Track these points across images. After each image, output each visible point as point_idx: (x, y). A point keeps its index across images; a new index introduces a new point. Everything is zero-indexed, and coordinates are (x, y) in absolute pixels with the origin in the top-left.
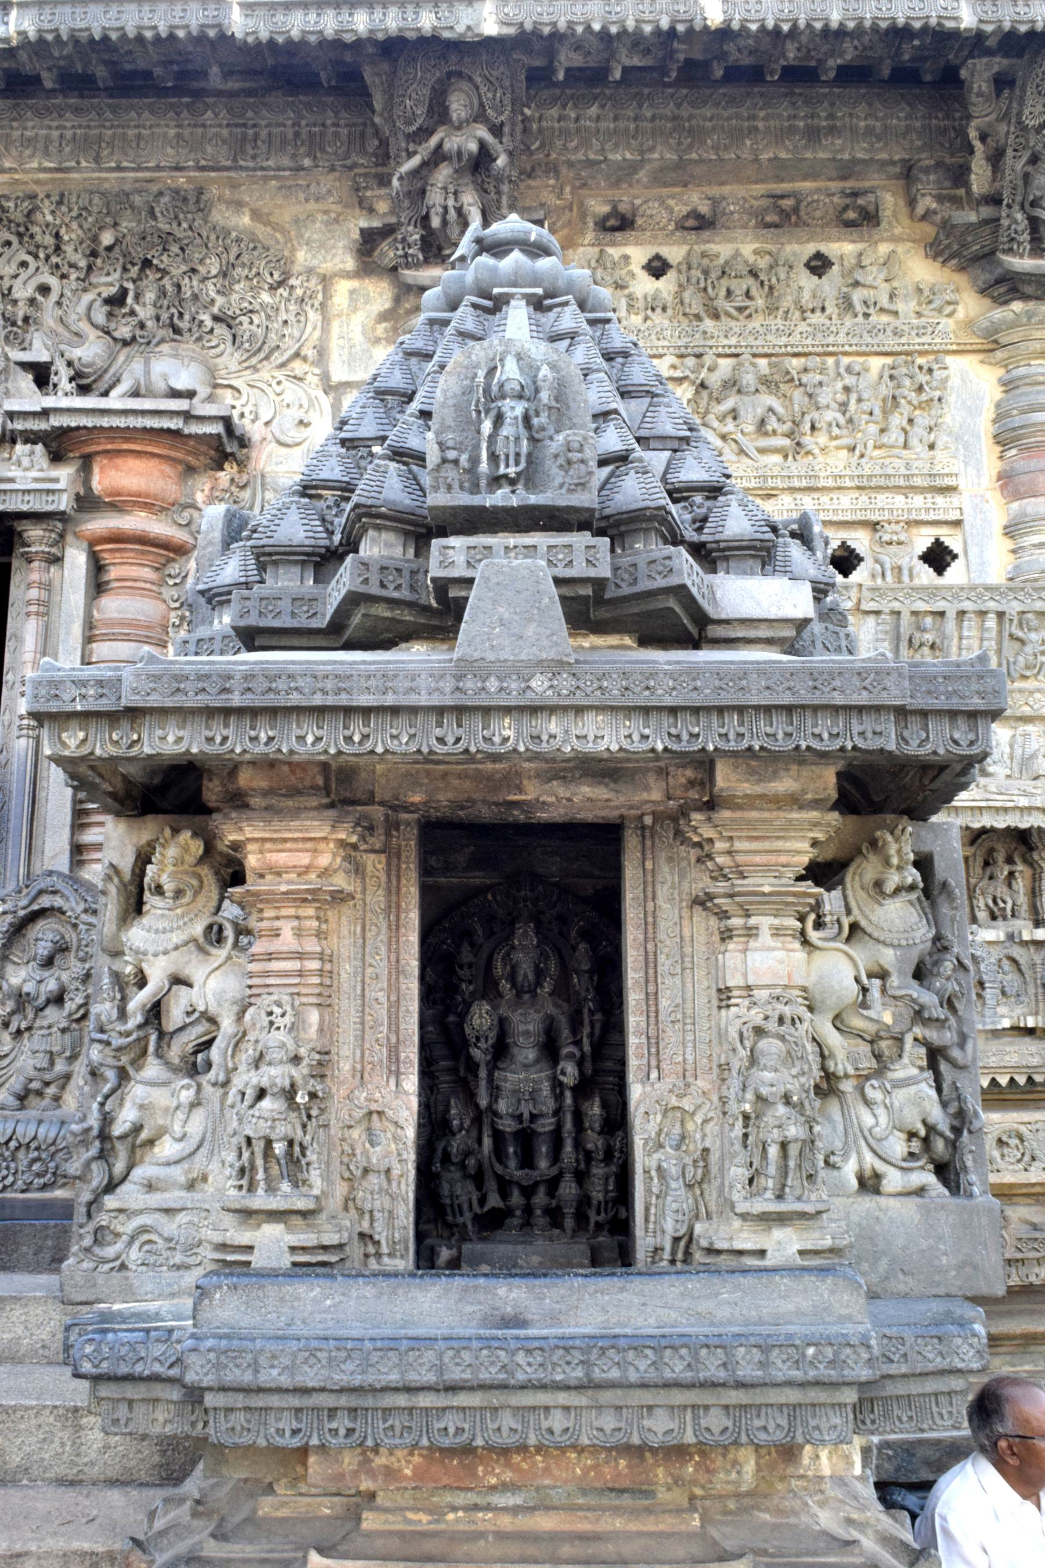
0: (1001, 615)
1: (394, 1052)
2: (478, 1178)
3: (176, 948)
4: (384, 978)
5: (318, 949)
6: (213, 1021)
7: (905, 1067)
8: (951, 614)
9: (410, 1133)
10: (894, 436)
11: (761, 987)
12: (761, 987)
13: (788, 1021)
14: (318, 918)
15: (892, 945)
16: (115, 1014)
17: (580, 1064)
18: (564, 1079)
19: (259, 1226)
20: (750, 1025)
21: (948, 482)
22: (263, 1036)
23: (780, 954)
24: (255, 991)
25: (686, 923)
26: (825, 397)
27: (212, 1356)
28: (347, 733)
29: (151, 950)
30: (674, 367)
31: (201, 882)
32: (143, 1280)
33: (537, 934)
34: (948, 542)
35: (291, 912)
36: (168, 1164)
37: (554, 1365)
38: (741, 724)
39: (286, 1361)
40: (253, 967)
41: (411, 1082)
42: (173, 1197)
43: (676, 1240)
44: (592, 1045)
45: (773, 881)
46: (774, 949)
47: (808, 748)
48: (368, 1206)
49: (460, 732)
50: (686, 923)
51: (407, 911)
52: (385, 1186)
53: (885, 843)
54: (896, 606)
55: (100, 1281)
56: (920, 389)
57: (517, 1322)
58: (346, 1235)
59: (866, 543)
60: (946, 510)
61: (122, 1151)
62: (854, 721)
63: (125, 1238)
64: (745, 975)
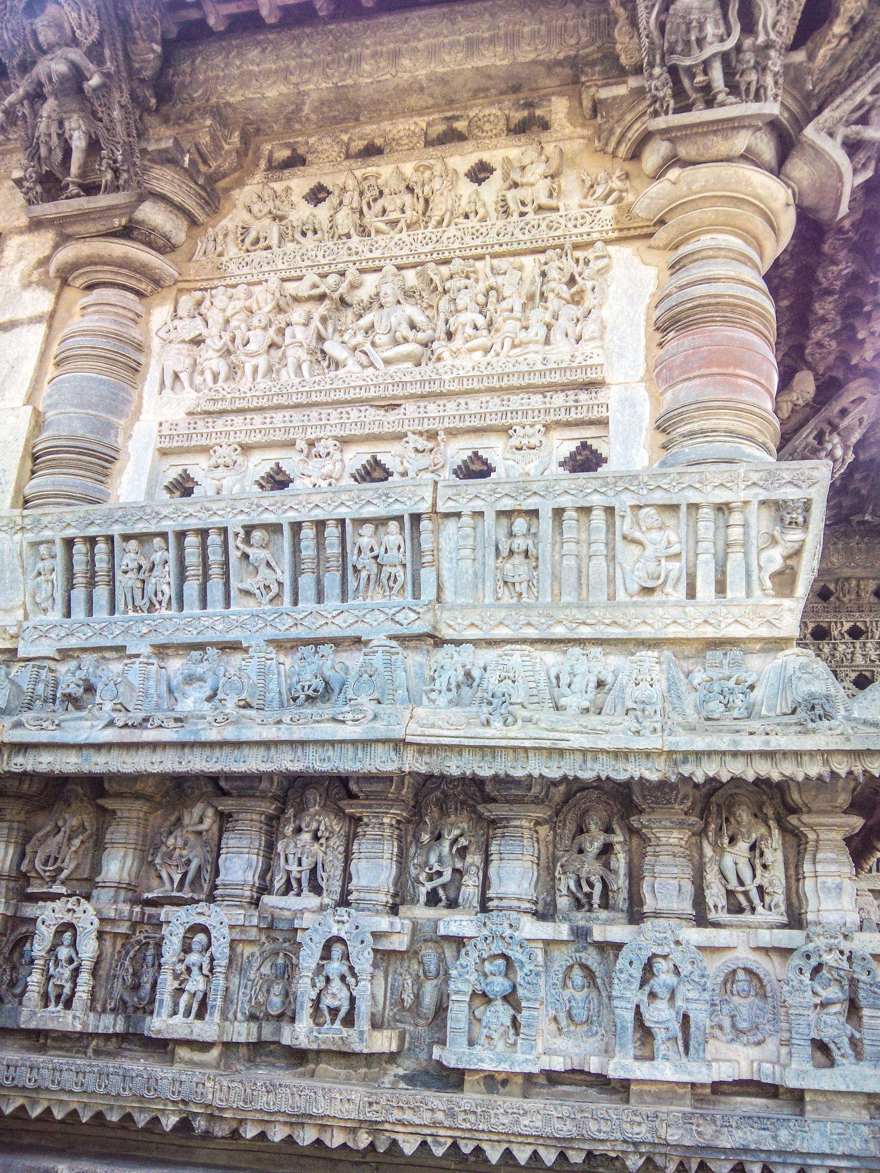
0: (610, 511)
8: (546, 514)
10: (537, 331)
21: (592, 376)
26: (463, 299)
30: (315, 286)
34: (595, 444)
54: (478, 505)
56: (572, 281)
59: (499, 451)
60: (590, 408)
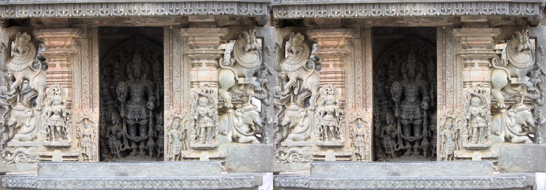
1: (91, 101)
2: (122, 139)
3: (24, 69)
4: (88, 78)
5: (67, 70)
6: (36, 91)
7: (248, 105)
9: (97, 125)
11: (202, 82)
12: (202, 82)
13: (209, 92)
14: (67, 61)
15: (246, 68)
16: (6, 90)
17: (155, 103)
18: (150, 108)
19: (53, 150)
20: (197, 93)
22: (52, 97)
23: (209, 72)
24: (49, 83)
25: (182, 61)
27: (44, 182)
28: (75, 10)
29: (16, 70)
31: (30, 48)
32: (20, 166)
33: (141, 58)
35: (59, 59)
36: (25, 134)
37: (134, 184)
38: (191, 7)
39: (63, 183)
40: (48, 76)
41: (97, 110)
42: (27, 143)
43: (176, 156)
44: (160, 96)
45: (207, 49)
46: (206, 70)
47: (211, 14)
48: (84, 146)
49: (108, 9)
50: (182, 61)
51: (95, 57)
52: (89, 140)
53: (246, 35)
55: (8, 166)
57: (125, 174)
58: (78, 153)
61: (11, 130)
62: (225, 6)
63: (14, 155)
64: (197, 78)
